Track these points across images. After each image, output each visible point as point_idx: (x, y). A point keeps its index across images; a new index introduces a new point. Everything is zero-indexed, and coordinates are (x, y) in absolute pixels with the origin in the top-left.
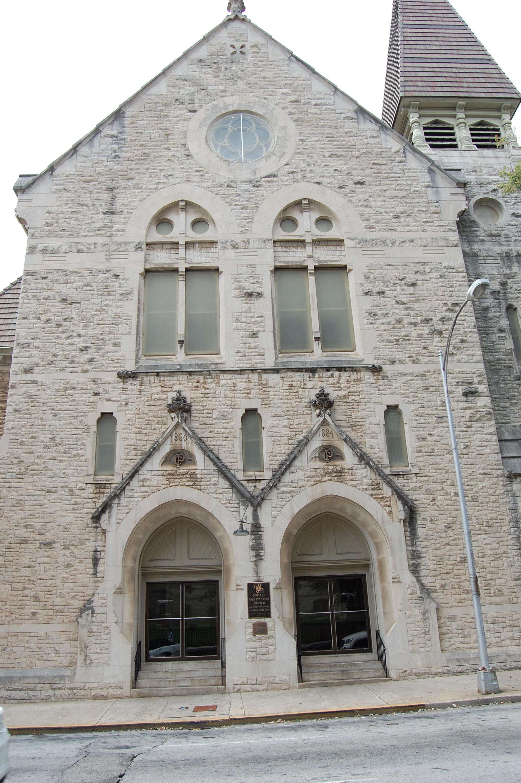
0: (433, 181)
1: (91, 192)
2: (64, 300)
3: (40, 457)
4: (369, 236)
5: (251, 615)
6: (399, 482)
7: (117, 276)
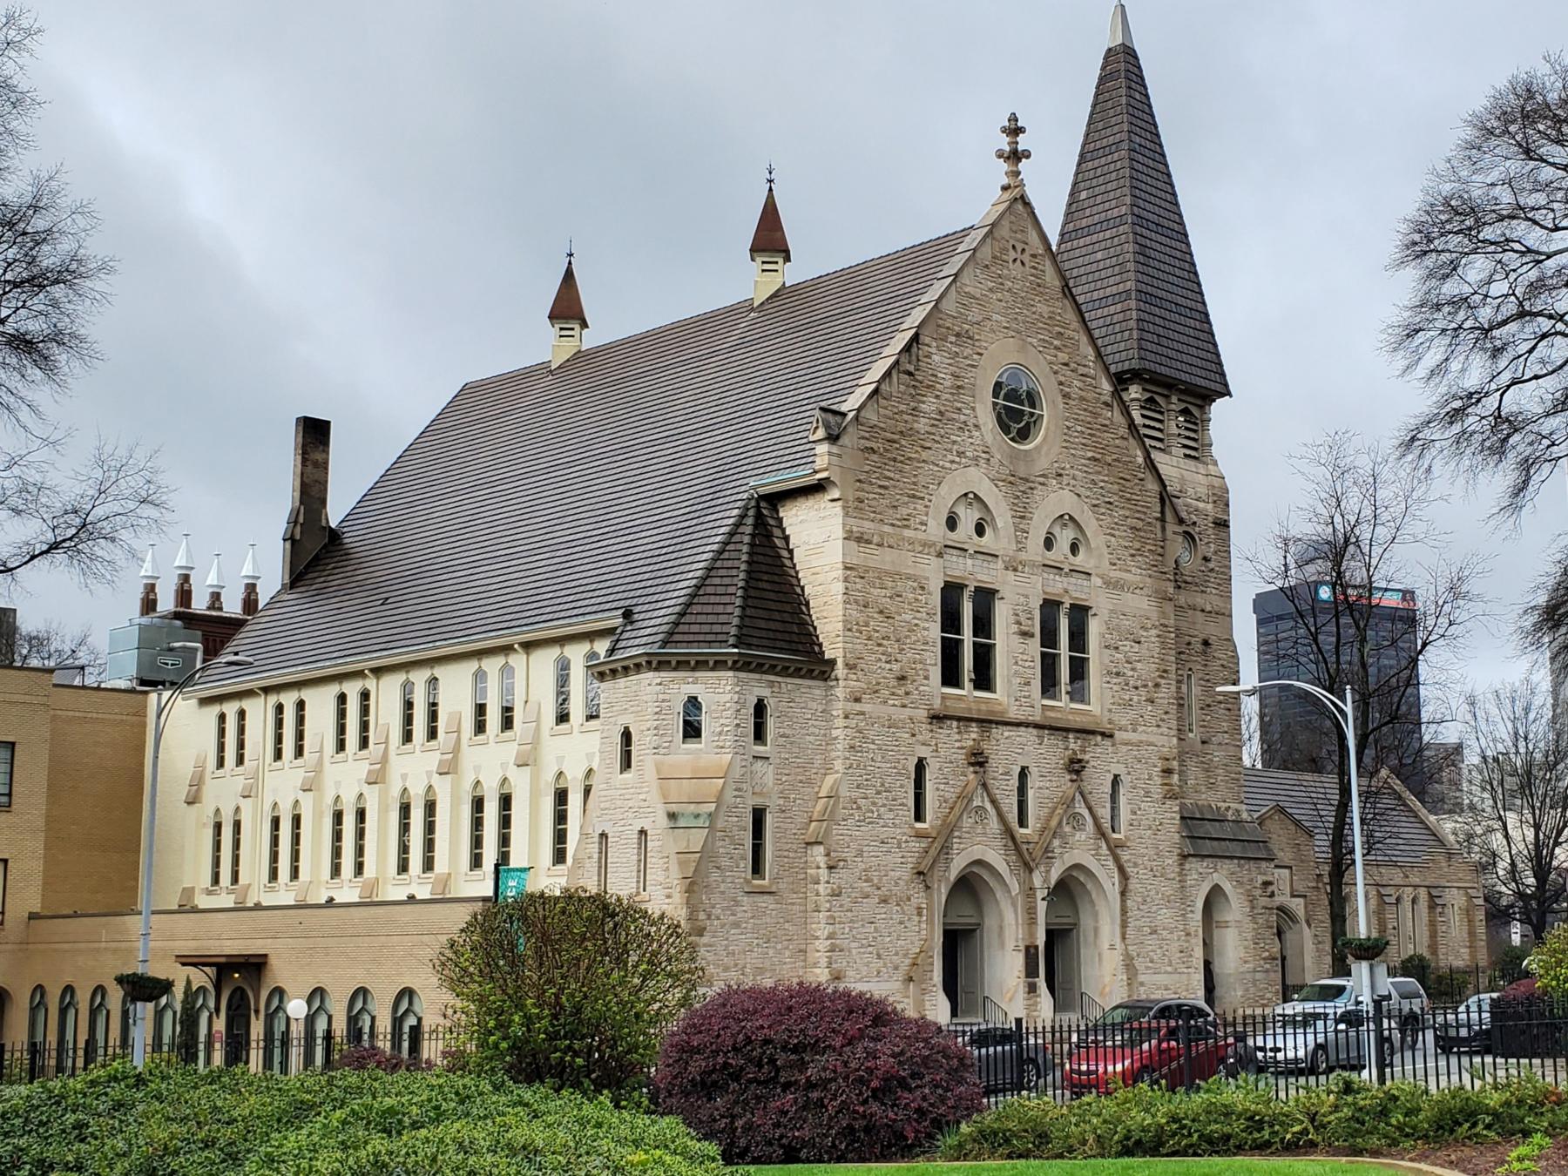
0: (1162, 512)
1: (895, 460)
2: (881, 612)
3: (874, 804)
4: (1115, 574)
5: (1027, 976)
6: (1119, 851)
7: (923, 588)
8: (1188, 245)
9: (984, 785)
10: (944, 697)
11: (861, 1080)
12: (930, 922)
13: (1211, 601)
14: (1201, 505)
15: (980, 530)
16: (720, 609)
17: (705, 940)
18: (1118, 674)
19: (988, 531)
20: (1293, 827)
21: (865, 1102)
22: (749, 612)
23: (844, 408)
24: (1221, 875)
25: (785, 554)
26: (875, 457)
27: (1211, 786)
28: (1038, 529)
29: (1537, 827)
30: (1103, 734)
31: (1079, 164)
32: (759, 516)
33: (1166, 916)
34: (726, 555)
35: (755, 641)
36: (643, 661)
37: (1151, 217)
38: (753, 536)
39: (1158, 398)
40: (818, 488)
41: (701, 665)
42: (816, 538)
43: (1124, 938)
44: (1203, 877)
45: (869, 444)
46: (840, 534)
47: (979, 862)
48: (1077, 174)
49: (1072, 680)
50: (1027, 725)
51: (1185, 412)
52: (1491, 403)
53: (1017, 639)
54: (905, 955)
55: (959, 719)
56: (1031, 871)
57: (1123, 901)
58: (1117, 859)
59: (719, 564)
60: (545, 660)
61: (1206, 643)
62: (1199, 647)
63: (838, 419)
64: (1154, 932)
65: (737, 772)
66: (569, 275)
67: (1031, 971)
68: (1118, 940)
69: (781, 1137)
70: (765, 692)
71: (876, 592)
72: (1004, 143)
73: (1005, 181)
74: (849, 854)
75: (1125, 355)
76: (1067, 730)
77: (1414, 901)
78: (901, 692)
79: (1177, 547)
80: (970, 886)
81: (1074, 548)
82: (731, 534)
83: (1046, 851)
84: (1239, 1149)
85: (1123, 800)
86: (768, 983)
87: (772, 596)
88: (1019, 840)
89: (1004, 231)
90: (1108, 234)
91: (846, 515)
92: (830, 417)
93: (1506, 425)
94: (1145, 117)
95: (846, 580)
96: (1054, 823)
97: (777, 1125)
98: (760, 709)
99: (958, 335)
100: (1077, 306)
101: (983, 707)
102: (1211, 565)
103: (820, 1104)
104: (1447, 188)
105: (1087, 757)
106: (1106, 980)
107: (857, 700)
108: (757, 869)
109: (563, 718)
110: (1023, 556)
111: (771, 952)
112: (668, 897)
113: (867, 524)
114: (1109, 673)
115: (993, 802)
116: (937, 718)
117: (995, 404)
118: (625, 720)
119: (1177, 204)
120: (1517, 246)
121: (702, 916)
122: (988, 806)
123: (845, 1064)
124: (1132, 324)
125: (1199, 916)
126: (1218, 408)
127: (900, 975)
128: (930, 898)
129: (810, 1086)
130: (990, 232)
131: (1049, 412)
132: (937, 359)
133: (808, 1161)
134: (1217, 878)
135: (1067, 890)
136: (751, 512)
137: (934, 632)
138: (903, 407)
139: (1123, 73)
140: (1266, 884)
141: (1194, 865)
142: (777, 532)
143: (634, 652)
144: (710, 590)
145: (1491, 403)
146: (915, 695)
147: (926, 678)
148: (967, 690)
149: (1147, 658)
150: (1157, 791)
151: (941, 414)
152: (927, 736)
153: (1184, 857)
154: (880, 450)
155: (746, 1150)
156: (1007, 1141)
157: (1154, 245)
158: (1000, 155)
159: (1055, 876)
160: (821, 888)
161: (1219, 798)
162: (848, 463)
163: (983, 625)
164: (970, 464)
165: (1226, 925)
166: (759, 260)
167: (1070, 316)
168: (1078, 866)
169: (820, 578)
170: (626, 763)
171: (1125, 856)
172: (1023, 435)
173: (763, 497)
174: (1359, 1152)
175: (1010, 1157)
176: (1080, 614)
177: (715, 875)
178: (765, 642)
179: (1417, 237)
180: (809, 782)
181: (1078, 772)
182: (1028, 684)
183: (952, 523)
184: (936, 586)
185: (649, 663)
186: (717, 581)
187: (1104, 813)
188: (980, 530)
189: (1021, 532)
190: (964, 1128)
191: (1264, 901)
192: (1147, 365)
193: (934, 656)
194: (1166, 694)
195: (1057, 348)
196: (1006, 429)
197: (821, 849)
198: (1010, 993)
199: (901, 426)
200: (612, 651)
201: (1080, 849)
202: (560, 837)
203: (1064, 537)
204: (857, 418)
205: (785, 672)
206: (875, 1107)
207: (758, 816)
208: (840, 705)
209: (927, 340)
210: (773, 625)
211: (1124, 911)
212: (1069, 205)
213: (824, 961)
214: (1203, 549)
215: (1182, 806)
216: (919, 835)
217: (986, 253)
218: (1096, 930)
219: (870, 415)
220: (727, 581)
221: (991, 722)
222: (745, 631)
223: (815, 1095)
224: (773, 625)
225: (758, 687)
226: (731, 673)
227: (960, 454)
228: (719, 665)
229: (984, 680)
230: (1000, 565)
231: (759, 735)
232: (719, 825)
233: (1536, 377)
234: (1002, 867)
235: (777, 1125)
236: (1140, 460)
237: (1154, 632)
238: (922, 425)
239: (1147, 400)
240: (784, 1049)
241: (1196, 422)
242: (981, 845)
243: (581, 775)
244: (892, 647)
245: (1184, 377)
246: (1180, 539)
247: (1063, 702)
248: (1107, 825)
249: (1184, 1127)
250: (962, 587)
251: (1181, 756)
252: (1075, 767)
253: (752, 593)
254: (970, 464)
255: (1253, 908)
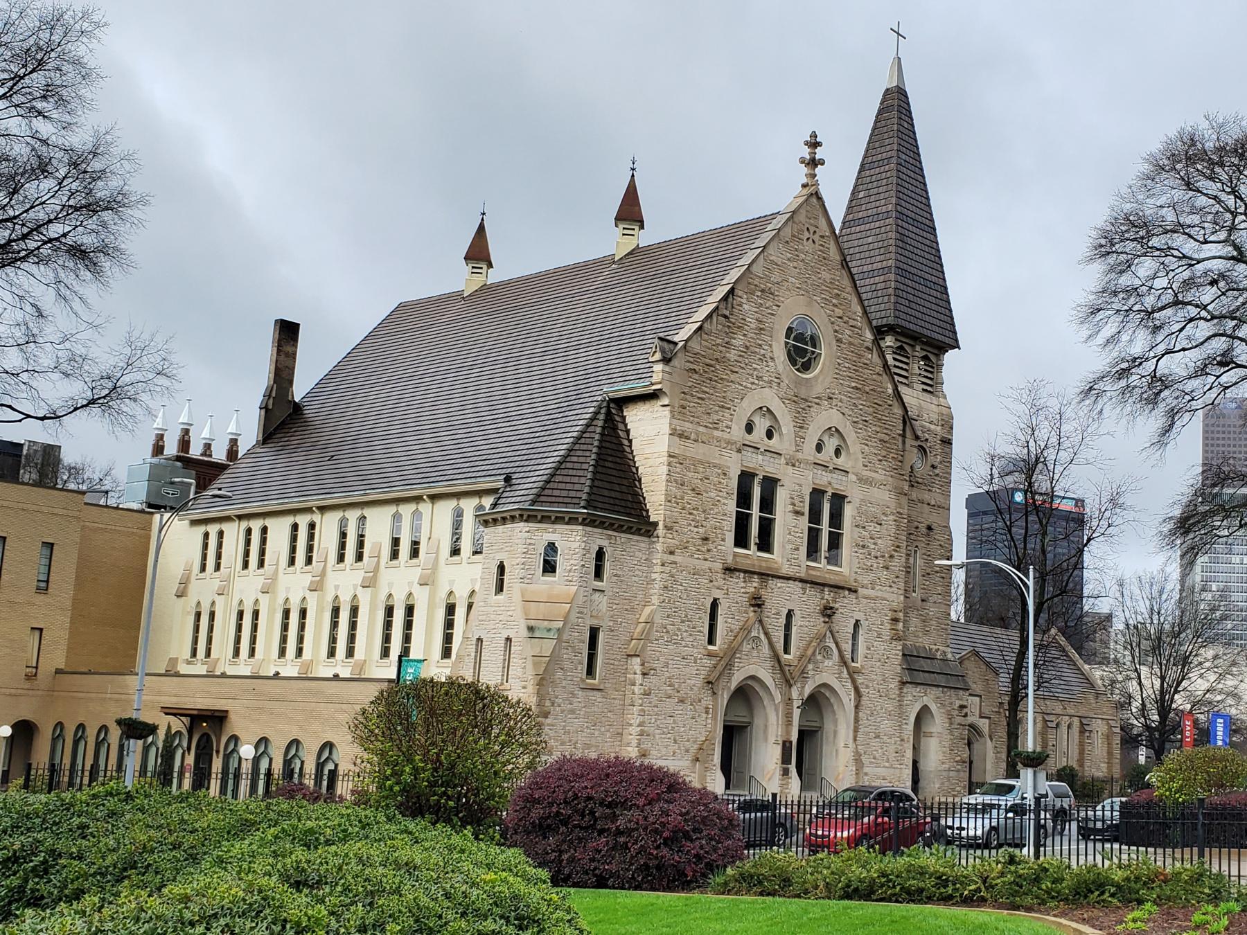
0: (904, 430)
1: (710, 379)
4: (867, 473)
6: (855, 676)
8: (936, 236)
9: (760, 621)
10: (735, 555)
11: (656, 831)
12: (714, 718)
13: (934, 497)
14: (933, 427)
15: (770, 435)
16: (576, 480)
17: (548, 721)
18: (863, 546)
19: (776, 435)
20: (984, 667)
21: (658, 847)
22: (596, 483)
23: (676, 339)
24: (929, 698)
25: (626, 442)
26: (696, 376)
27: (926, 633)
28: (812, 435)
29: (1163, 678)
30: (850, 590)
31: (860, 172)
32: (609, 413)
33: (887, 726)
34: (583, 441)
35: (600, 505)
36: (517, 514)
37: (909, 214)
38: (603, 428)
39: (906, 347)
40: (653, 396)
41: (559, 520)
42: (649, 431)
43: (855, 740)
44: (916, 699)
45: (692, 366)
46: (667, 430)
47: (753, 678)
48: (857, 179)
49: (830, 548)
50: (795, 579)
51: (925, 358)
52: (1149, 366)
53: (792, 516)
54: (695, 742)
55: (745, 572)
56: (790, 686)
57: (856, 713)
58: (854, 682)
59: (577, 447)
60: (445, 509)
61: (929, 528)
62: (924, 531)
63: (671, 346)
64: (877, 737)
65: (581, 600)
66: (481, 228)
67: (786, 759)
68: (851, 741)
69: (595, 868)
70: (605, 543)
71: (691, 474)
72: (806, 152)
73: (805, 180)
74: (658, 665)
75: (884, 313)
76: (824, 585)
77: (1069, 727)
78: (704, 549)
79: (913, 457)
80: (745, 695)
81: (838, 452)
82: (588, 426)
83: (803, 672)
84: (929, 900)
85: (861, 639)
86: (593, 755)
87: (615, 473)
88: (783, 662)
89: (801, 217)
90: (877, 225)
91: (673, 417)
92: (665, 345)
93: (1159, 383)
94: (911, 141)
95: (669, 464)
96: (810, 652)
97: (592, 860)
98: (600, 555)
99: (763, 291)
100: (852, 275)
101: (764, 564)
102: (937, 471)
103: (625, 846)
104: (1127, 207)
105: (837, 606)
106: (839, 770)
107: (672, 553)
108: (590, 671)
109: (456, 552)
110: (800, 456)
111: (597, 733)
112: (524, 688)
113: (687, 425)
114: (857, 545)
115: (766, 634)
116: (729, 570)
117: (787, 343)
118: (501, 556)
119: (929, 206)
120: (1176, 253)
121: (548, 703)
122: (762, 637)
123: (646, 818)
124: (891, 291)
125: (911, 727)
126: (950, 357)
127: (690, 756)
128: (715, 701)
129: (619, 832)
130: (792, 217)
131: (826, 352)
132: (747, 307)
133: (614, 888)
134: (926, 700)
135: (816, 702)
136: (603, 411)
137: (731, 507)
138: (719, 341)
139: (896, 107)
140: (962, 707)
141: (911, 691)
142: (621, 426)
143: (511, 507)
144: (569, 465)
145: (1149, 366)
146: (714, 552)
147: (723, 540)
148: (752, 551)
149: (886, 535)
150: (886, 634)
151: (747, 347)
152: (720, 582)
153: (903, 683)
154: (701, 371)
155: (569, 876)
156: (760, 882)
157: (911, 235)
158: (802, 161)
159: (808, 691)
160: (636, 689)
161: (931, 642)
162: (676, 379)
163: (768, 504)
164: (764, 388)
165: (930, 735)
166: (621, 226)
167: (846, 282)
168: (825, 685)
169: (650, 462)
170: (500, 588)
171: (860, 680)
172: (806, 367)
173: (612, 400)
174: (1016, 907)
175: (761, 894)
176: (838, 500)
177: (559, 674)
178: (607, 506)
179: (1103, 241)
180: (632, 611)
181: (829, 616)
182: (797, 549)
183: (749, 428)
184: (735, 473)
185: (521, 516)
186: (575, 459)
187: (847, 647)
188: (770, 435)
189: (800, 438)
190: (729, 871)
191: (959, 719)
192: (900, 322)
193: (730, 525)
194: (898, 563)
195: (834, 305)
196: (793, 362)
197: (638, 660)
198: (769, 774)
199: (717, 355)
200: (494, 505)
201: (827, 673)
202: (448, 639)
203: (831, 444)
204: (685, 347)
205: (620, 529)
206: (665, 851)
207: (594, 633)
208: (659, 556)
209: (740, 293)
210: (613, 494)
211: (857, 720)
212: (851, 201)
213: (635, 743)
214: (931, 460)
215: (904, 646)
216: (711, 655)
217: (787, 232)
218: (835, 732)
219: (695, 345)
220: (582, 460)
221: (768, 575)
222: (593, 497)
223: (622, 839)
224: (613, 494)
225: (600, 538)
226: (580, 527)
227: (758, 378)
228: (572, 520)
229: (765, 544)
230: (783, 461)
231: (598, 574)
232: (565, 637)
233: (1184, 349)
234: (769, 682)
235: (592, 860)
236: (890, 391)
237: (892, 517)
238: (732, 355)
239: (898, 348)
240: (601, 804)
241: (932, 365)
242: (755, 665)
243: (466, 594)
244: (700, 516)
245: (926, 332)
246: (916, 450)
247: (822, 564)
248: (848, 656)
249: (890, 881)
250: (753, 475)
251: (906, 609)
252: (828, 612)
253: (600, 469)
254: (764, 388)
255: (951, 724)
